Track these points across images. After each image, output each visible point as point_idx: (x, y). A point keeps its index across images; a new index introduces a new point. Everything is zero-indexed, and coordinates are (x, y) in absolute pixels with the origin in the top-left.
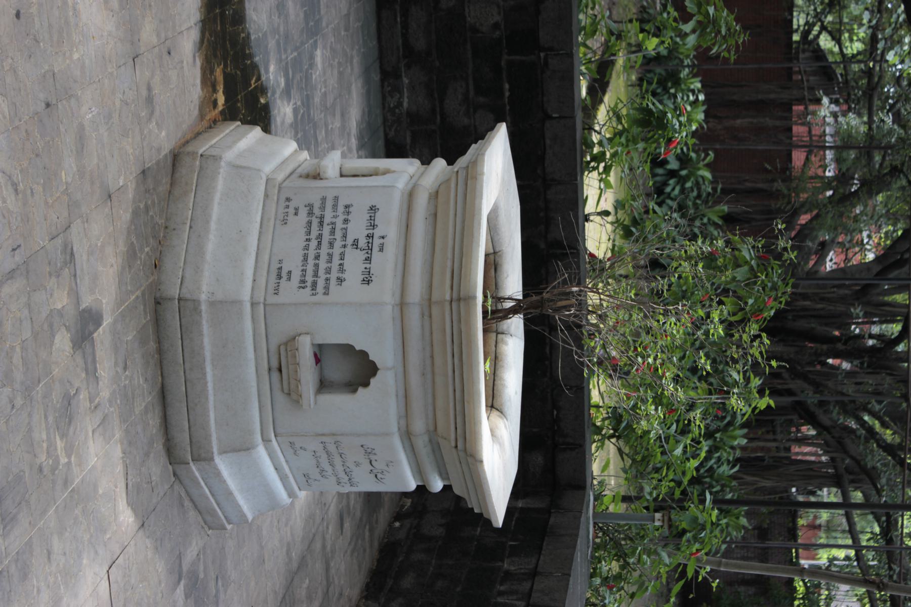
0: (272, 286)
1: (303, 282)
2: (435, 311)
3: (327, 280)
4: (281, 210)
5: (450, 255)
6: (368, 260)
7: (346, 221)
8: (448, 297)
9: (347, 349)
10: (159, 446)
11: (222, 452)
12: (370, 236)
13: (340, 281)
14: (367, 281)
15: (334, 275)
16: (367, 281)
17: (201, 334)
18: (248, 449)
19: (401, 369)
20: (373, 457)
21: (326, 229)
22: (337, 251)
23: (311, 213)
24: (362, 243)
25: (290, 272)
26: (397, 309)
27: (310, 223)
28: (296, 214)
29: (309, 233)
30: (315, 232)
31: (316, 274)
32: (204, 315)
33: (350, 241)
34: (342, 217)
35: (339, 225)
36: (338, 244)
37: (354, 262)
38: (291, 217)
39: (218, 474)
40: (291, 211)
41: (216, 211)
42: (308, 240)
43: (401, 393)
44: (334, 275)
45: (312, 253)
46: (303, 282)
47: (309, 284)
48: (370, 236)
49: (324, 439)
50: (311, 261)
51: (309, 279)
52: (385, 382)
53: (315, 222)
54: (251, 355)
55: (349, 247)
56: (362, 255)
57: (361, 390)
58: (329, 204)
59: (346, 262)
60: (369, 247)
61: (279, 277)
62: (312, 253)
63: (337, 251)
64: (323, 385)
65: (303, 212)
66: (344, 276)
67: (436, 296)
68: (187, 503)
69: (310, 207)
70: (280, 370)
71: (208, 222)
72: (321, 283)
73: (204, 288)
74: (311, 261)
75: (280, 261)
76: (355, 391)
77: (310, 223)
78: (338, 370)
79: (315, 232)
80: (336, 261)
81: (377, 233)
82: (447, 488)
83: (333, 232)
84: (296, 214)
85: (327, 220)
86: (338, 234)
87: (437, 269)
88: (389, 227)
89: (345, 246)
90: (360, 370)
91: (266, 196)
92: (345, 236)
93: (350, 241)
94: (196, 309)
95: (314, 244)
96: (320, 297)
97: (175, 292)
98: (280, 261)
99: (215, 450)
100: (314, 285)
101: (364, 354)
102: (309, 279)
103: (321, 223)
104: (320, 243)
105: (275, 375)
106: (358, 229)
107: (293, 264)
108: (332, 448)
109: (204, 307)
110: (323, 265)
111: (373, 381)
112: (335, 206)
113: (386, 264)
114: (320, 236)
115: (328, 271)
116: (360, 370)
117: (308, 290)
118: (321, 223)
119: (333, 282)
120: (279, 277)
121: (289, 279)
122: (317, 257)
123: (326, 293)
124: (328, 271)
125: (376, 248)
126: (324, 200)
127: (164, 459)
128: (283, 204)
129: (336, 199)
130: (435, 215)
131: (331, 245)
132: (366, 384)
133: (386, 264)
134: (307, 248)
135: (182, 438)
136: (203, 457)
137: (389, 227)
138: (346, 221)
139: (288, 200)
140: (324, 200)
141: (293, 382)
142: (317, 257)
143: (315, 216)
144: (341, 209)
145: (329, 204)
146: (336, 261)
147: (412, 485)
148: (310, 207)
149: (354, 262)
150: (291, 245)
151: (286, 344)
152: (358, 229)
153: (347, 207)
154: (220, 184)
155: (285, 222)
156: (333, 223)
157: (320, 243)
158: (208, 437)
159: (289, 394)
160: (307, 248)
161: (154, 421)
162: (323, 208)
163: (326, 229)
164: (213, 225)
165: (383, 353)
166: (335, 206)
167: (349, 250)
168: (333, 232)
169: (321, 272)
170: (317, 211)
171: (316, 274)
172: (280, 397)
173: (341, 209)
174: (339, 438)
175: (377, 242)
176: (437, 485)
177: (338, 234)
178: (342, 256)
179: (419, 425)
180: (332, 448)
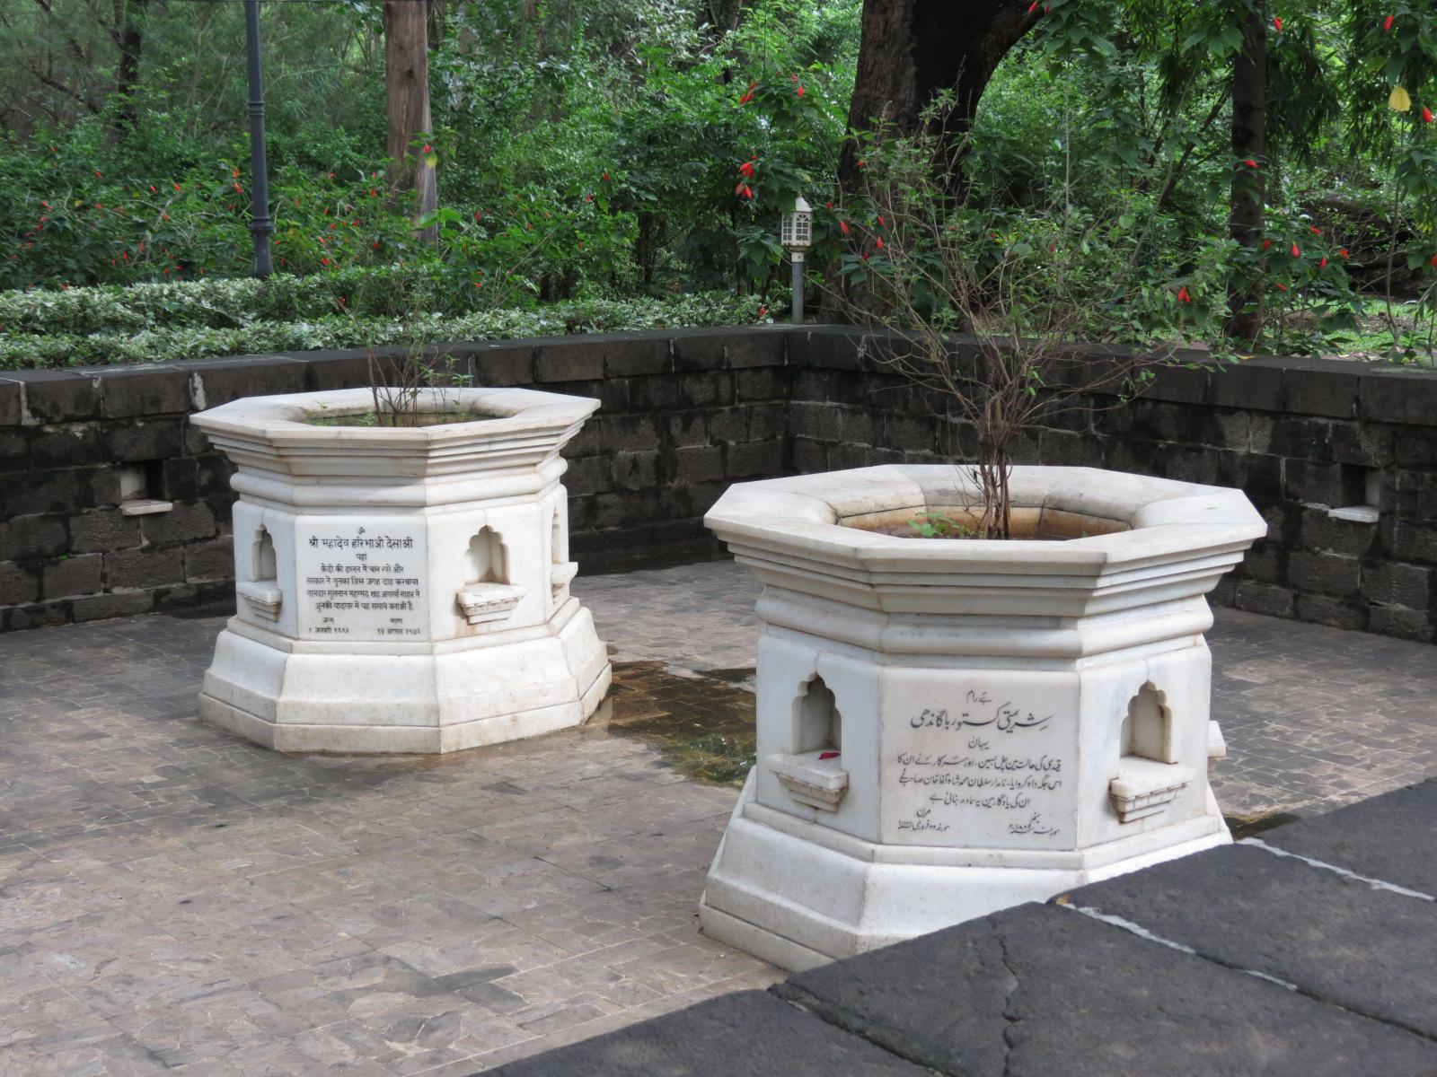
1: (403, 606)
13: (398, 569)
21: (342, 587)
23: (327, 605)
25: (393, 620)
29: (350, 605)
30: (349, 599)
31: (396, 594)
33: (359, 563)
44: (393, 575)
45: (372, 600)
47: (405, 600)
51: (400, 600)
53: (338, 599)
55: (366, 562)
62: (372, 600)
65: (327, 613)
66: (393, 566)
72: (404, 588)
74: (382, 600)
76: (503, 549)
77: (337, 605)
79: (349, 599)
83: (344, 581)
89: (365, 567)
92: (355, 569)
93: (359, 563)
95: (361, 599)
98: (381, 631)
100: (409, 594)
102: (400, 600)
106: (347, 556)
110: (382, 588)
114: (353, 593)
121: (400, 620)
123: (416, 582)
126: (311, 593)
129: (310, 580)
134: (366, 606)
140: (311, 593)
142: (375, 594)
157: (362, 593)
162: (321, 593)
163: (342, 587)
165: (470, 521)
168: (344, 581)
171: (396, 594)
178: (374, 569)
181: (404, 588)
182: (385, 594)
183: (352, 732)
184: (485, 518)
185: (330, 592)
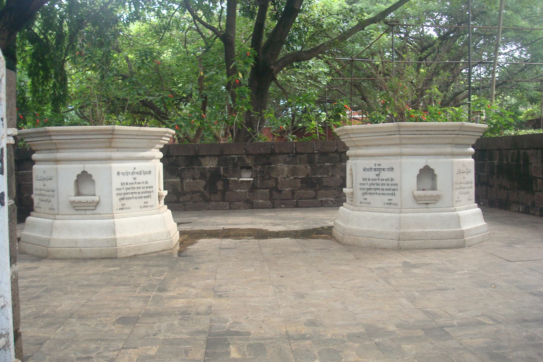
0: (394, 206)
1: (392, 194)
2: (404, 141)
3: (392, 185)
4: (365, 205)
5: (382, 137)
6: (384, 169)
7: (369, 180)
8: (398, 136)
9: (418, 176)
10: (458, 250)
11: (460, 227)
12: (375, 170)
13: (392, 180)
14: (392, 169)
15: (390, 182)
16: (392, 169)
17: (413, 232)
18: (459, 217)
19: (427, 157)
20: (461, 171)
21: (372, 187)
22: (380, 182)
23: (366, 194)
24: (377, 172)
25: (389, 200)
26: (403, 157)
27: (370, 194)
28: (366, 199)
31: (390, 189)
32: (405, 231)
33: (377, 177)
34: (368, 181)
35: (371, 182)
36: (378, 182)
37: (385, 175)
38: (368, 201)
39: (469, 230)
40: (365, 201)
41: (365, 228)
42: (376, 193)
43: (436, 157)
44: (390, 182)
45: (381, 192)
46: (392, 194)
47: (393, 192)
48: (375, 170)
49: (454, 188)
50: (385, 192)
51: (391, 192)
52: (431, 162)
53: (370, 191)
54: (422, 214)
56: (382, 173)
57: (436, 172)
58: (362, 187)
59: (385, 178)
60: (379, 170)
61: (390, 204)
62: (381, 192)
63: (380, 182)
64: (434, 188)
65: (366, 196)
67: (398, 142)
68: (480, 244)
69: (363, 194)
70: (427, 204)
71: (369, 231)
72: (393, 187)
73: (395, 231)
74: (385, 192)
75: (384, 204)
77: (370, 194)
78: (427, 183)
80: (384, 182)
81: (373, 167)
82: (473, 146)
83: (373, 184)
84: (366, 199)
85: (368, 187)
86: (374, 182)
87: (387, 142)
88: (371, 163)
90: (427, 173)
91: (359, 210)
92: (375, 180)
93: (377, 177)
94: (403, 234)
95: (378, 191)
96: (398, 187)
97: (396, 242)
98: (384, 204)
99: (459, 229)
100: (394, 190)
101: (421, 170)
102: (391, 192)
103: (370, 189)
104: (377, 189)
105: (429, 206)
107: (385, 199)
108: (458, 186)
109: (402, 231)
110: (386, 187)
111: (431, 168)
112: (364, 184)
113: (385, 163)
114: (375, 189)
115: (388, 185)
116: (427, 173)
117: (396, 192)
118: (370, 189)
119: (392, 182)
120: (390, 204)
122: (383, 189)
123: (397, 185)
124: (388, 185)
125: (380, 167)
126: (361, 189)
127: (464, 249)
128: (362, 205)
129: (360, 184)
130: (367, 146)
131: (378, 184)
132: (433, 170)
133: (385, 163)
134: (379, 194)
135: (454, 242)
136: (461, 235)
137: (371, 163)
138: (369, 180)
139: (361, 203)
140: (361, 189)
141: (432, 199)
142: (383, 189)
143: (368, 192)
144: (364, 182)
145: (362, 187)
146: (384, 182)
147: (471, 161)
148: (363, 194)
149: (385, 175)
150: (378, 200)
151: (417, 201)
152: (372, 175)
153: (364, 180)
154: (354, 227)
155: (369, 203)
156: (370, 184)
157: (377, 189)
158: (454, 232)
159: (437, 200)
160: (379, 194)
161: (448, 251)
162: (364, 189)
163: (372, 187)
164: (370, 229)
165: (421, 162)
166: (364, 184)
167: (380, 178)
168: (373, 184)
169: (388, 187)
170: (365, 191)
171: (390, 189)
172: (439, 204)
173: (364, 182)
174: (454, 182)
175: (377, 167)
176: (472, 150)
177: (374, 182)
178: (382, 180)
179: (449, 149)
180: (458, 186)
181: (393, 187)
182: (386, 189)
183: (145, 245)
184: (427, 161)
185: (368, 189)
